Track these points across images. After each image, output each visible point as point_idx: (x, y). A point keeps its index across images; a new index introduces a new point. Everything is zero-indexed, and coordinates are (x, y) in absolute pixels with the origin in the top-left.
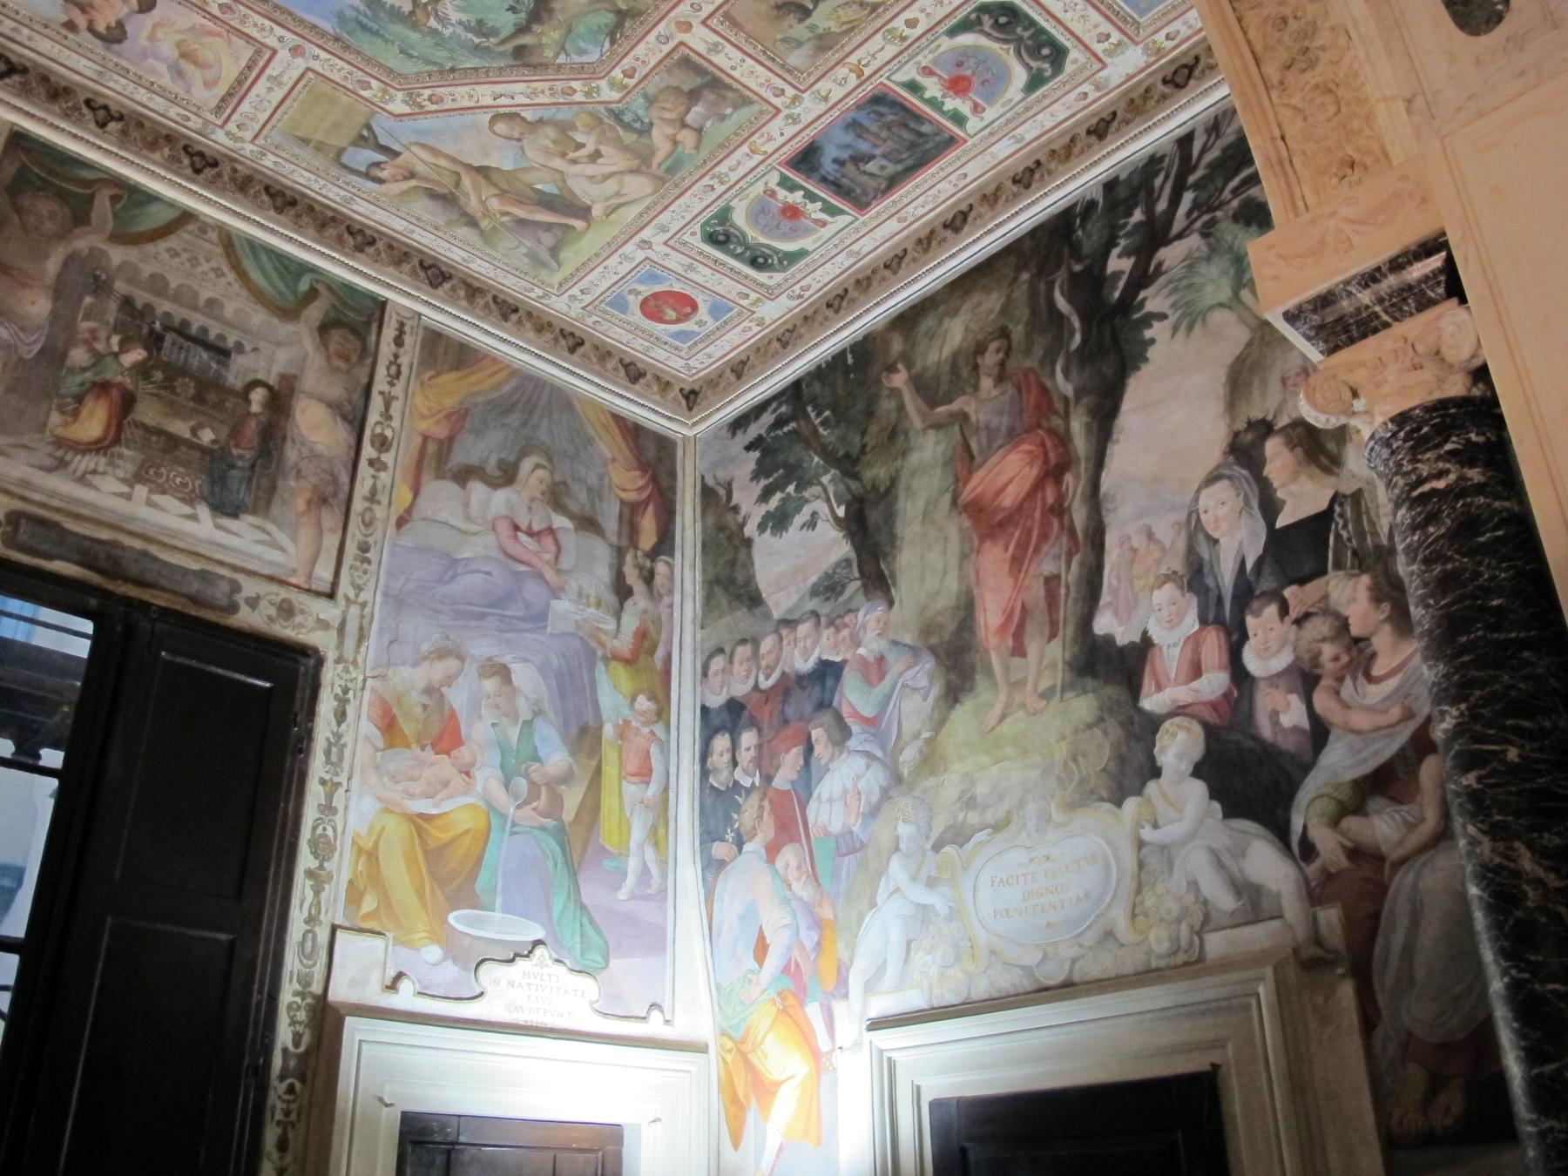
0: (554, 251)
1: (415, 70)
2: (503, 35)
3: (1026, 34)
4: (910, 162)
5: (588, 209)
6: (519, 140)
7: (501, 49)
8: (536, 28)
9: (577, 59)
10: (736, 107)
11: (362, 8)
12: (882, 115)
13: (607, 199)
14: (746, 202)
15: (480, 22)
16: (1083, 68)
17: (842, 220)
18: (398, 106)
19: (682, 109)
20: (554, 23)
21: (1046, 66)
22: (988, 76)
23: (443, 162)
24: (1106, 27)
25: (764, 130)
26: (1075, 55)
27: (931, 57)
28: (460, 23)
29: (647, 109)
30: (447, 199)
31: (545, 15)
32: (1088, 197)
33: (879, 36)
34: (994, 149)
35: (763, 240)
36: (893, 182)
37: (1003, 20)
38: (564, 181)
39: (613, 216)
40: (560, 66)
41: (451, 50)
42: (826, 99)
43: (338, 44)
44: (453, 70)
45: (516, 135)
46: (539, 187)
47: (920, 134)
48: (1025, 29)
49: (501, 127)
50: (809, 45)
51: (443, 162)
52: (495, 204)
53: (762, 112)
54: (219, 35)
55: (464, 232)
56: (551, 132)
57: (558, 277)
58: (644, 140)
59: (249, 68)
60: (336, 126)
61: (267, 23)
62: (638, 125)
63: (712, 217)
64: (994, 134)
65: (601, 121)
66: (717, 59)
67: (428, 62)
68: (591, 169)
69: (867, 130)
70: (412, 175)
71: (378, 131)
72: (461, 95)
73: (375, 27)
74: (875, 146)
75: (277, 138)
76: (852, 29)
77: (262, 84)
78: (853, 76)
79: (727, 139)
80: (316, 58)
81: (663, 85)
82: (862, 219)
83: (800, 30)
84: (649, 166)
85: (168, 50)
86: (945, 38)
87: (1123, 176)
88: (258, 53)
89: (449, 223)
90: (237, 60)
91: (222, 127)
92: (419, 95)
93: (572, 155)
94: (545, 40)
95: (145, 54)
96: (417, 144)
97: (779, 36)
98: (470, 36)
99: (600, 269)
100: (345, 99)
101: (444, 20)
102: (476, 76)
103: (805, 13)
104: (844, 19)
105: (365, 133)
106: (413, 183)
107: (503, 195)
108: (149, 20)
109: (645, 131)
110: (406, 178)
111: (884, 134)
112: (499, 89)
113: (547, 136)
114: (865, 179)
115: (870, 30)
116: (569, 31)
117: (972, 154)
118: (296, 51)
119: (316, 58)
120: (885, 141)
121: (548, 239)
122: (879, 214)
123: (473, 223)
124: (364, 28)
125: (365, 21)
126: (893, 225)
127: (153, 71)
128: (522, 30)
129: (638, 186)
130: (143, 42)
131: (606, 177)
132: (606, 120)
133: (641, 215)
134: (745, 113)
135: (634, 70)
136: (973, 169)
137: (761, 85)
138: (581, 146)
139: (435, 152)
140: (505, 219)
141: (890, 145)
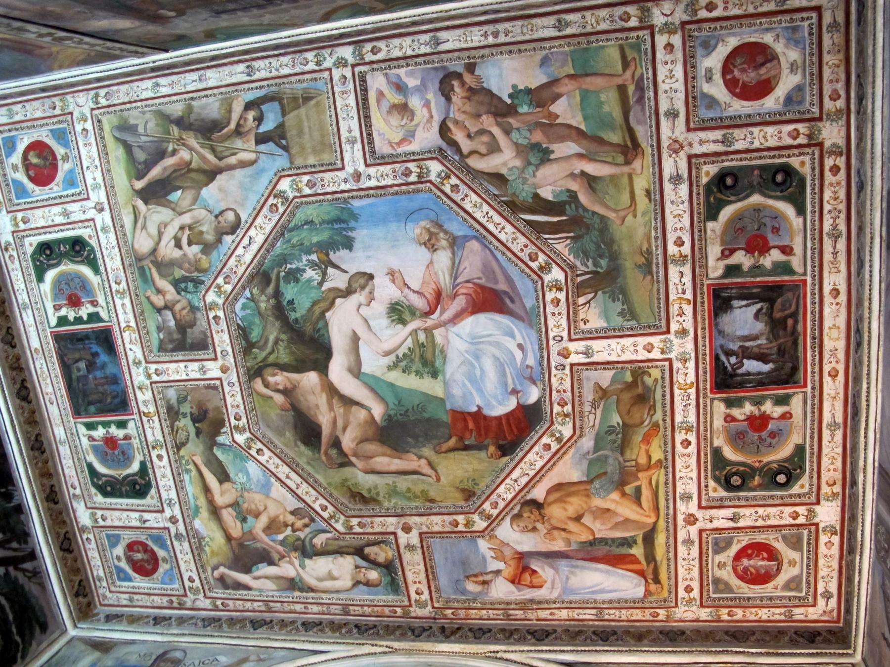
0: (128, 148)
1: (297, 215)
2: (282, 281)
3: (124, 489)
4: (75, 384)
5: (146, 203)
6: (216, 217)
7: (275, 271)
8: (272, 301)
9: (242, 301)
10: (161, 342)
11: (350, 234)
12: (114, 398)
13: (145, 218)
14: (96, 285)
15: (297, 280)
16: (90, 496)
17: (54, 322)
18: (285, 185)
19: (178, 316)
20: (270, 313)
21: (100, 483)
22: (109, 457)
23: (232, 160)
24: (108, 523)
25: (139, 344)
26: (99, 499)
27: (136, 446)
28: (304, 271)
29: (190, 303)
30: (209, 130)
31: (277, 313)
32: (16, 493)
33: (161, 439)
34: (62, 429)
35: (62, 268)
36: (66, 368)
37: (137, 487)
38: (173, 210)
39: (131, 210)
40: (245, 289)
41: (294, 246)
42: (140, 388)
43: (341, 198)
44: (283, 234)
45: (220, 218)
46: (179, 192)
47: (90, 403)
48: (126, 490)
49: (230, 216)
50: (176, 405)
51: (232, 160)
52: (184, 154)
53: (151, 351)
54: (399, 144)
55: (177, 109)
56: (210, 237)
57: (107, 127)
58: (171, 278)
59: (370, 135)
60: (300, 133)
61: (384, 183)
62: (183, 285)
63: (95, 255)
64: (72, 436)
65: (198, 270)
66: (195, 366)
67: (297, 228)
68: (171, 232)
69: (107, 383)
70: (238, 132)
71: (280, 151)
72: (265, 225)
73: (336, 226)
74: (95, 378)
75: (320, 84)
76: (172, 430)
77: (356, 133)
78: (146, 411)
79: (144, 320)
80: (346, 181)
81: (198, 323)
82: (49, 331)
83: (186, 408)
84: (152, 262)
85: (415, 102)
86: (142, 459)
87: (22, 517)
88: (373, 152)
89: (190, 108)
90: (379, 135)
91: (353, 66)
92: (283, 203)
93: (187, 232)
94: (263, 298)
95: (423, 84)
96: (255, 161)
97: (189, 398)
98: (294, 266)
99: (97, 162)
100: (311, 160)
101: (312, 264)
102: (269, 243)
103: (195, 420)
104: (180, 431)
105: (284, 142)
106: (232, 126)
107: (185, 169)
108: (437, 119)
109: (176, 283)
110: (238, 125)
111: (101, 389)
112: (255, 247)
113: (208, 229)
114: (77, 356)
115: (168, 439)
116: (259, 313)
117: (64, 418)
118: (357, 176)
119: (346, 181)
120: (96, 385)
121: (141, 156)
122: (48, 343)
123: (182, 123)
124: (339, 220)
125: (343, 225)
126: (35, 343)
127: (411, 74)
128: (277, 294)
129: (144, 244)
130: (430, 96)
131: (160, 234)
132: (196, 274)
133: (122, 226)
134: (155, 343)
135: (217, 324)
136: (54, 410)
137: (167, 369)
138: (190, 243)
139: (243, 164)
140: (170, 148)
141: (91, 385)
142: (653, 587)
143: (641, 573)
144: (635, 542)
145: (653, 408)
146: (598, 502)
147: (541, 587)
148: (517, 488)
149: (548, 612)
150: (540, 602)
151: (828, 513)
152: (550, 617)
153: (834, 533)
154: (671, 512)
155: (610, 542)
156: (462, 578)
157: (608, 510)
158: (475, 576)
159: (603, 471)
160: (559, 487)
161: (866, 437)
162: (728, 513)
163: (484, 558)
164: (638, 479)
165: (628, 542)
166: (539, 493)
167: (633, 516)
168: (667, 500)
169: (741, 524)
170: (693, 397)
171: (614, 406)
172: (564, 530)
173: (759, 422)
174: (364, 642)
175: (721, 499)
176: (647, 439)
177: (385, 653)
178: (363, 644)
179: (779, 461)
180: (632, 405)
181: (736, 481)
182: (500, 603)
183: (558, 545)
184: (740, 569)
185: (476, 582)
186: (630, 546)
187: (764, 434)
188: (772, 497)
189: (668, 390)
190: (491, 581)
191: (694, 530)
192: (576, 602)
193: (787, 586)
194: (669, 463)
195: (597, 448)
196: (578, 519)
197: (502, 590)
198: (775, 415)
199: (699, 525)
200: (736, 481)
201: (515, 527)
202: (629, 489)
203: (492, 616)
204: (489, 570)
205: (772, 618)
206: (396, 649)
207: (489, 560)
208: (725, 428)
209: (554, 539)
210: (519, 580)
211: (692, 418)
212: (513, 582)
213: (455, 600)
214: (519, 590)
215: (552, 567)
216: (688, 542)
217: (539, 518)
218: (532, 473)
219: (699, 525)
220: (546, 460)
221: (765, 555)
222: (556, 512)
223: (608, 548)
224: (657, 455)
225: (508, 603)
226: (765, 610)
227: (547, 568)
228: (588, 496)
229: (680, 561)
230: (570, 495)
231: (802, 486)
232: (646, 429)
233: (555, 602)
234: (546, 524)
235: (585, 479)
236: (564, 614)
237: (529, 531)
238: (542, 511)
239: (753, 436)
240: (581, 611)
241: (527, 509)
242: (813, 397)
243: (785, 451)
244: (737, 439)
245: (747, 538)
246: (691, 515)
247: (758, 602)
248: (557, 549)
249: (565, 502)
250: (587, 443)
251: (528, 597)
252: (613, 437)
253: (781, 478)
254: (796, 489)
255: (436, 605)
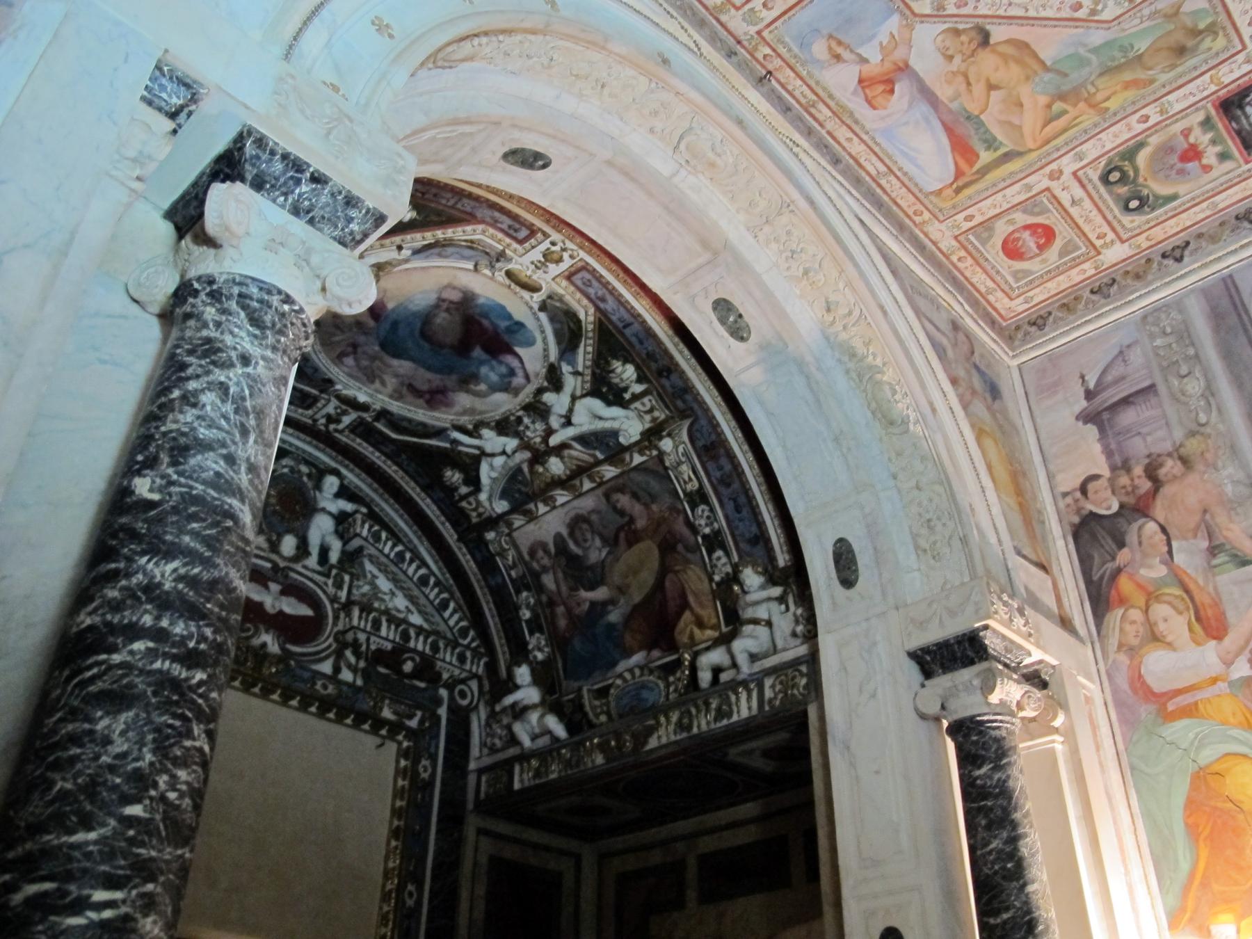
142: (949, 192)
143: (959, 174)
144: (995, 150)
145: (1173, 67)
146: (1025, 92)
147: (874, 108)
148: (1001, 12)
149: (850, 135)
150: (857, 122)
151: (1115, 254)
152: (842, 140)
153: (1096, 268)
154: (1055, 155)
155: (982, 130)
156: (825, 32)
157: (1021, 105)
158: (840, 43)
159: (1067, 71)
160: (1023, 46)
161: (1242, 247)
162: (1078, 192)
163: (874, 36)
164: (1075, 105)
165: (991, 143)
166: (999, 33)
167: (1027, 130)
168: (1066, 144)
169: (1074, 211)
170: (1206, 93)
171: (1159, 33)
172: (969, 84)
173: (1192, 154)
174: (675, 14)
175: (1090, 181)
176: (1127, 86)
177: (690, 49)
178: (672, 16)
179: (1151, 191)
180: (1170, 48)
181: (1115, 176)
182: (824, 89)
183: (944, 92)
184: (1017, 235)
185: (830, 48)
186: (988, 148)
187: (1180, 165)
188: (1112, 210)
189: (1204, 68)
190: (845, 61)
191: (1046, 183)
192: (882, 149)
193: (1016, 275)
194: (1109, 119)
195: (1095, 50)
196: (991, 87)
197: (841, 80)
198: (1205, 161)
199: (1054, 185)
200: (1115, 176)
201: (940, 38)
202: (1058, 106)
203: (797, 93)
204: (859, 51)
205: (978, 285)
206: (701, 55)
207: (876, 42)
208: (1175, 135)
209: (949, 82)
210: (868, 87)
211: (1178, 107)
212: (860, 81)
213: (785, 45)
214: (855, 93)
215: (910, 106)
216: (1029, 187)
217: (968, 53)
218: (1032, 13)
219: (1054, 185)
220: (1058, 16)
221: (1042, 241)
222: (987, 63)
223: (973, 132)
224: (1112, 105)
225: (831, 96)
226: (984, 276)
227: (906, 99)
228: (1027, 78)
229: (1000, 194)
230: (1018, 61)
231: (1132, 221)
232: (1143, 77)
233: (867, 133)
234: (964, 65)
235: (1049, 63)
236: (856, 148)
237: (943, 54)
238: (979, 50)
239: (1174, 159)
240: (874, 159)
241: (973, 34)
242: (1239, 176)
243: (1163, 190)
244: (1166, 149)
245: (1053, 220)
246: (1061, 172)
247: (989, 268)
248: (939, 93)
249: (1006, 62)
250: (1097, 37)
251: (851, 106)
252: (1117, 54)
253: (1134, 204)
254: (1127, 219)
255: (765, 34)
